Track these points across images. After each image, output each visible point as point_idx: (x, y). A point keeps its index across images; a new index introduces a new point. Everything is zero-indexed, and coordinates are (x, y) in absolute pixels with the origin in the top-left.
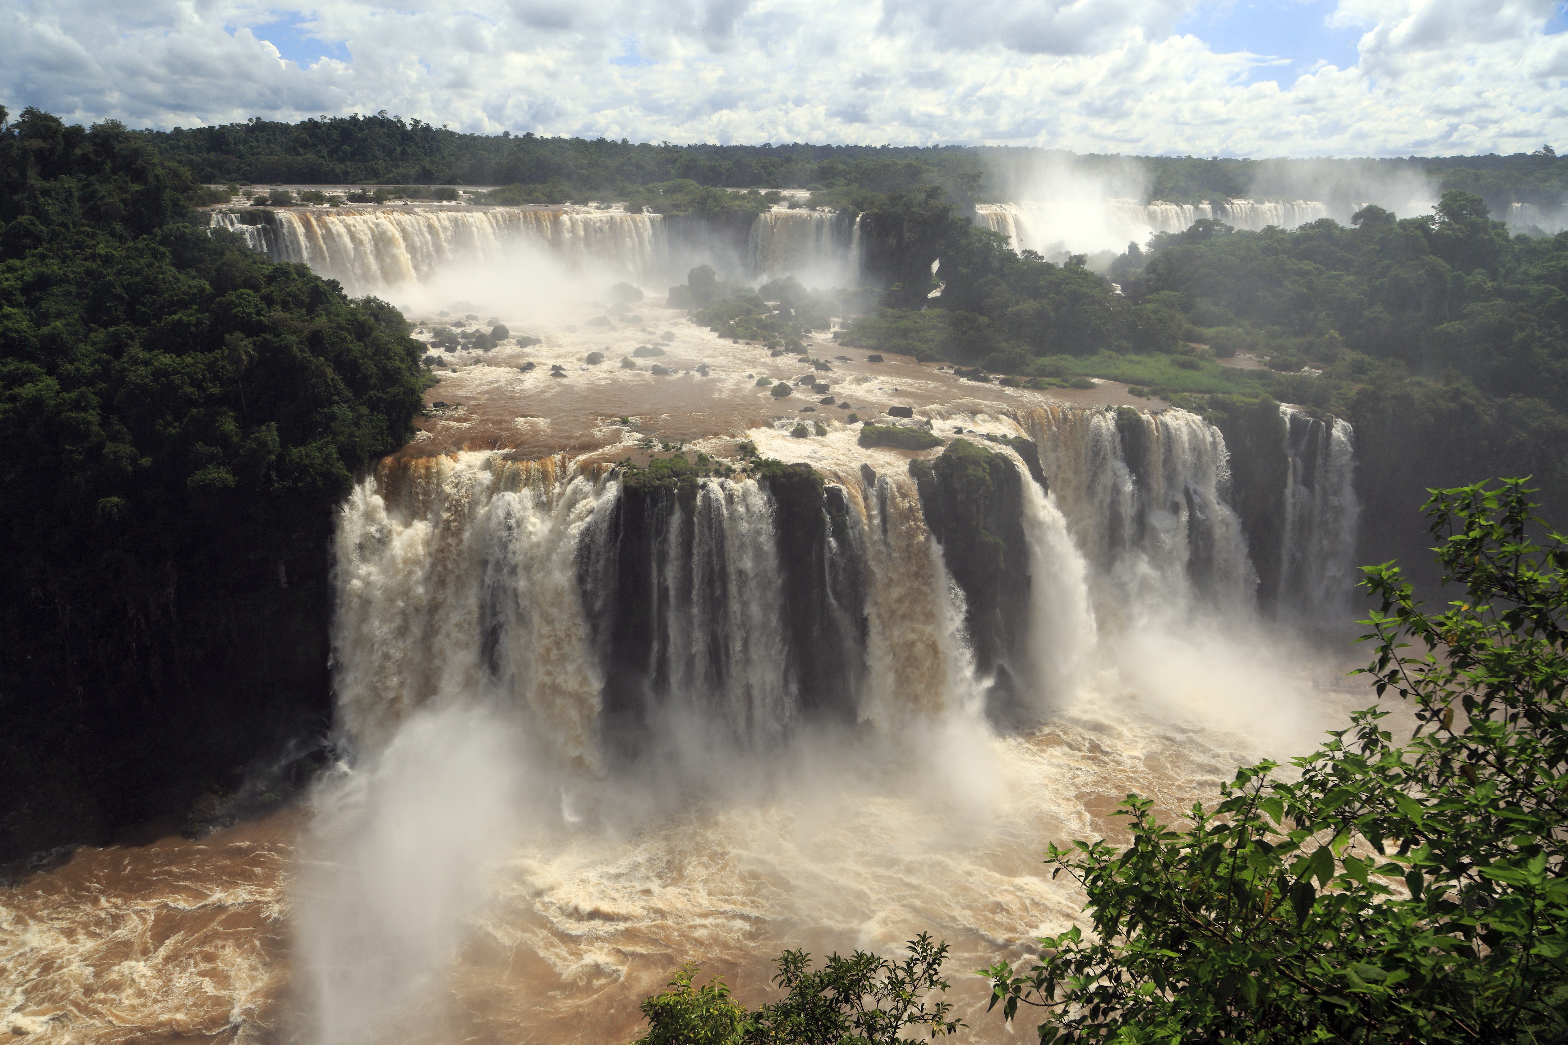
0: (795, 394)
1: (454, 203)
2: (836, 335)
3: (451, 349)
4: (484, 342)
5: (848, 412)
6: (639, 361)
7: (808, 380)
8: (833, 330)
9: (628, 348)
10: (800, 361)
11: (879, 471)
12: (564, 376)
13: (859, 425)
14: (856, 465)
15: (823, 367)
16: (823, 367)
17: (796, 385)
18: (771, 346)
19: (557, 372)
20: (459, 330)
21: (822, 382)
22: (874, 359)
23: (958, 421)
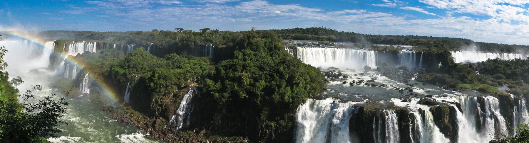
22: (424, 84)
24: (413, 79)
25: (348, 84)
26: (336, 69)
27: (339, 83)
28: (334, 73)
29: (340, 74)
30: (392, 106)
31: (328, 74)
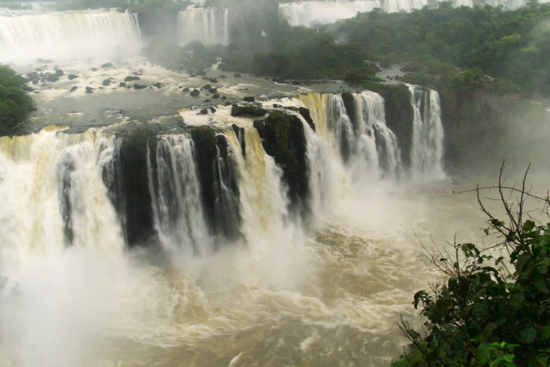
0: (202, 94)
1: (32, 11)
2: (220, 65)
3: (35, 83)
4: (53, 78)
5: (225, 101)
6: (127, 83)
7: (207, 87)
8: (218, 63)
9: (121, 78)
10: (204, 78)
11: (240, 126)
12: (92, 92)
13: (230, 107)
14: (230, 125)
15: (214, 81)
16: (214, 81)
17: (202, 90)
18: (189, 73)
19: (89, 90)
20: (39, 72)
21: (214, 87)
22: (237, 76)
23: (273, 102)
24: (215, 67)
25: (80, 92)
26: (49, 61)
27: (61, 92)
28: (44, 72)
29: (60, 73)
30: (181, 126)
31: (34, 77)
